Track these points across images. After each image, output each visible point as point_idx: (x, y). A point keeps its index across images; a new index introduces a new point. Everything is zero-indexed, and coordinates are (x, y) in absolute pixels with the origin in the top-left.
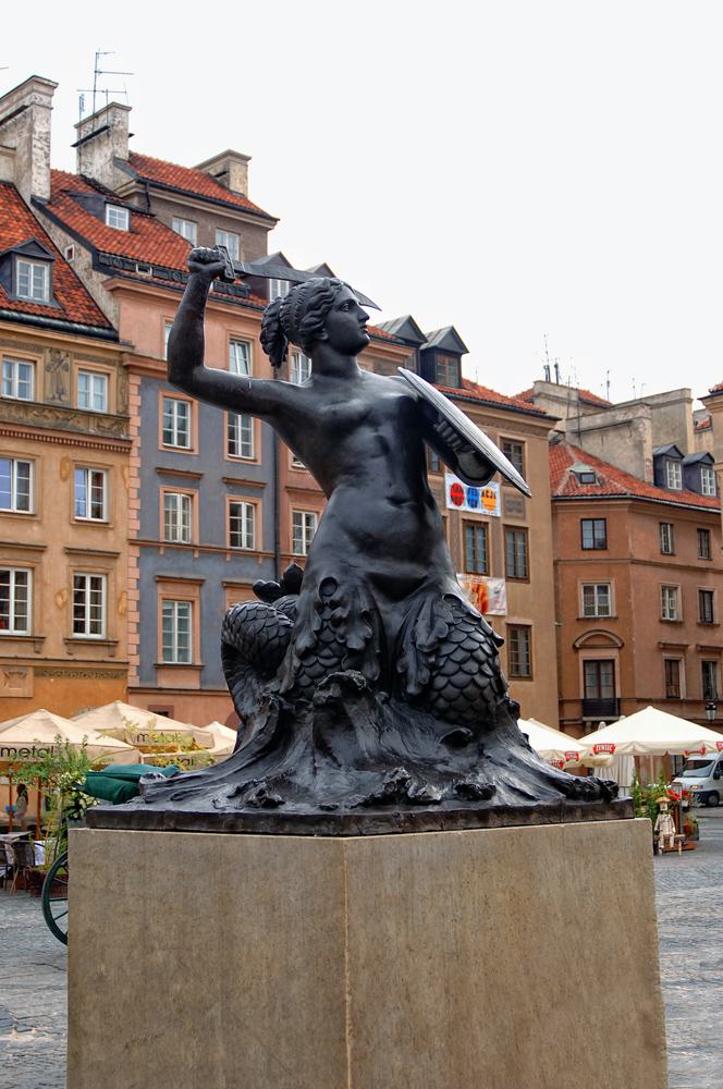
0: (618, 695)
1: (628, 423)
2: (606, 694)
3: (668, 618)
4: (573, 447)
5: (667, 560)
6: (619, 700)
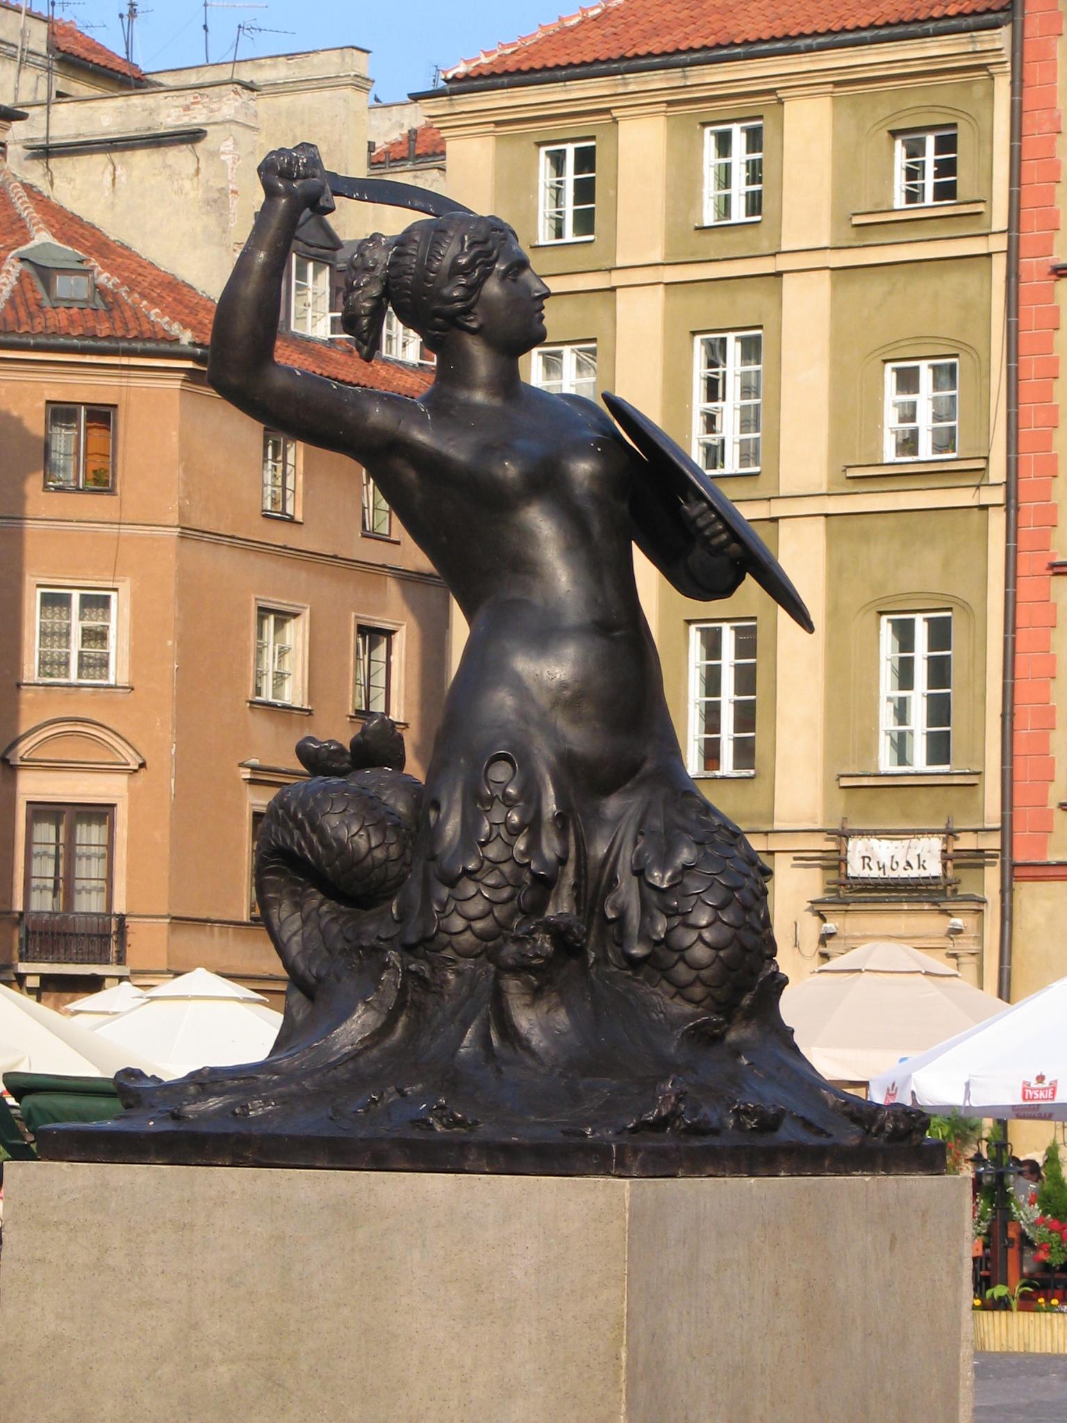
0: (119, 907)
1: (192, 136)
2: (89, 903)
3: (267, 696)
4: (28, 188)
5: (279, 535)
6: (122, 918)
